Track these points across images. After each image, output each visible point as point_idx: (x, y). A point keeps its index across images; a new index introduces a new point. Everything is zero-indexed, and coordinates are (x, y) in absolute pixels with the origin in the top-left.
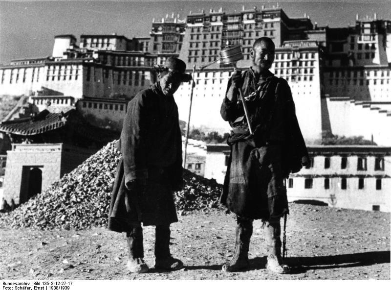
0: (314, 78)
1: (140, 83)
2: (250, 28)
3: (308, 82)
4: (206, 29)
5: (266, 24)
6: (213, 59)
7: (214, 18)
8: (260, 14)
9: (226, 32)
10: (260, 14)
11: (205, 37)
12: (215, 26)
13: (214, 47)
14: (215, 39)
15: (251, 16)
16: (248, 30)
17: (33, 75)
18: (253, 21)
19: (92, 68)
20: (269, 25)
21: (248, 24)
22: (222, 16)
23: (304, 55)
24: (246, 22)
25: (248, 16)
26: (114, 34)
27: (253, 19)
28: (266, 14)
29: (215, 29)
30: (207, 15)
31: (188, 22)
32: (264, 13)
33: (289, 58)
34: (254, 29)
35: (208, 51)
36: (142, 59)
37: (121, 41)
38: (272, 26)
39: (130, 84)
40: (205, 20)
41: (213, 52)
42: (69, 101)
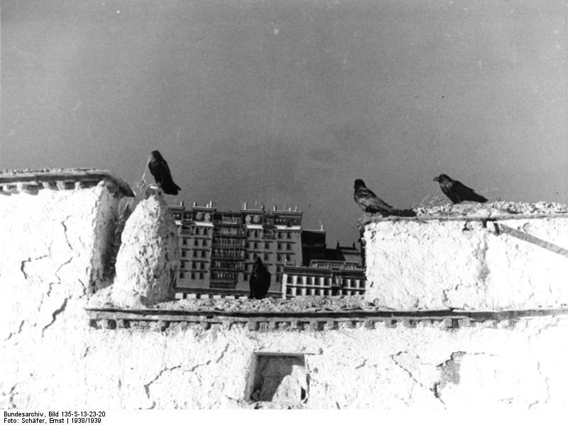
2: (256, 235)
4: (186, 230)
5: (280, 232)
6: (198, 275)
7: (199, 215)
8: (271, 217)
9: (219, 237)
10: (271, 217)
12: (202, 227)
14: (200, 246)
15: (256, 218)
16: (252, 237)
18: (260, 227)
20: (285, 235)
21: (252, 230)
22: (213, 213)
23: (349, 281)
24: (250, 227)
25: (252, 218)
27: (259, 223)
28: (279, 218)
29: (202, 231)
30: (188, 209)
32: (276, 216)
33: (326, 283)
34: (263, 238)
35: (191, 263)
38: (289, 237)
40: (185, 217)
41: (198, 265)
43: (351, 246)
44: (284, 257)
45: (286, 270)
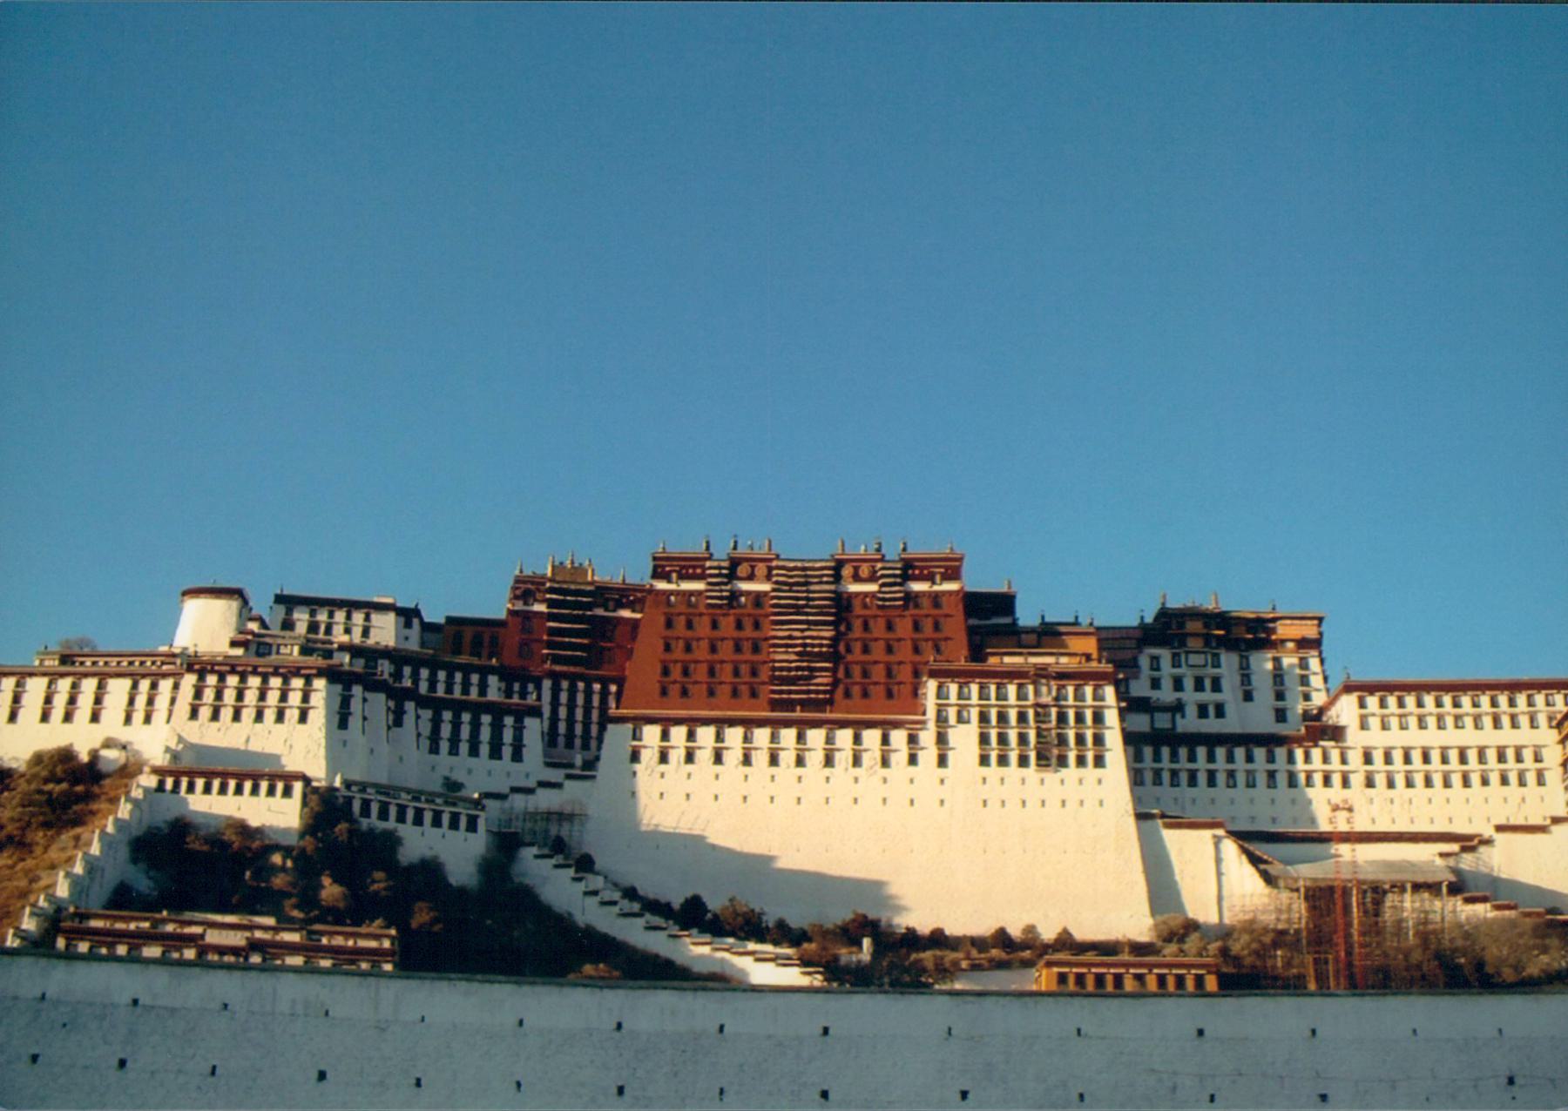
0: (1108, 757)
1: (507, 751)
3: (1090, 772)
7: (743, 570)
11: (715, 625)
13: (748, 656)
17: (131, 702)
18: (872, 587)
19: (357, 690)
21: (857, 594)
25: (856, 569)
26: (389, 600)
28: (914, 568)
31: (656, 575)
36: (493, 680)
37: (408, 625)
39: (474, 751)
42: (298, 787)
43: (1072, 620)
44: (927, 647)
45: (933, 674)
